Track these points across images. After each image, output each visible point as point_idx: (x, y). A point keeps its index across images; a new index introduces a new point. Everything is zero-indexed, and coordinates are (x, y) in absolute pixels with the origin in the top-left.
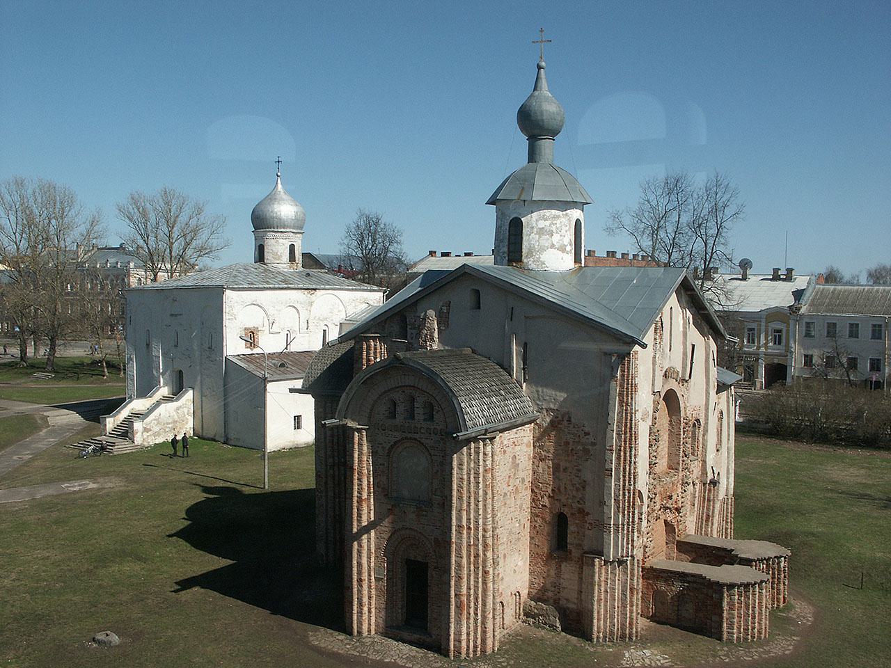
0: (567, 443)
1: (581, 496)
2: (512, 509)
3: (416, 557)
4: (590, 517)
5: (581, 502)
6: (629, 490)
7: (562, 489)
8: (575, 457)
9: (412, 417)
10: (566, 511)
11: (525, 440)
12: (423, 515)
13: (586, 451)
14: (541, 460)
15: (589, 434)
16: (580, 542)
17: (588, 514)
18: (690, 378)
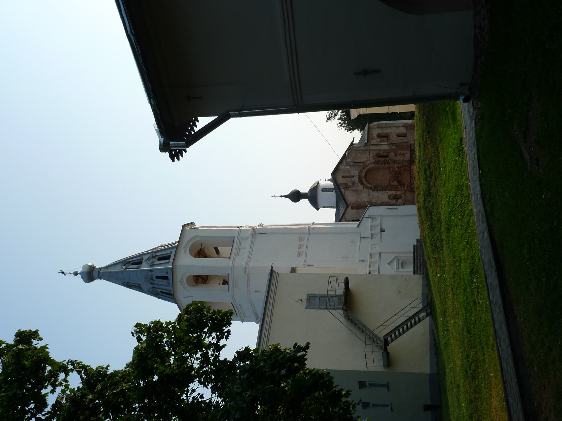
18: (363, 163)
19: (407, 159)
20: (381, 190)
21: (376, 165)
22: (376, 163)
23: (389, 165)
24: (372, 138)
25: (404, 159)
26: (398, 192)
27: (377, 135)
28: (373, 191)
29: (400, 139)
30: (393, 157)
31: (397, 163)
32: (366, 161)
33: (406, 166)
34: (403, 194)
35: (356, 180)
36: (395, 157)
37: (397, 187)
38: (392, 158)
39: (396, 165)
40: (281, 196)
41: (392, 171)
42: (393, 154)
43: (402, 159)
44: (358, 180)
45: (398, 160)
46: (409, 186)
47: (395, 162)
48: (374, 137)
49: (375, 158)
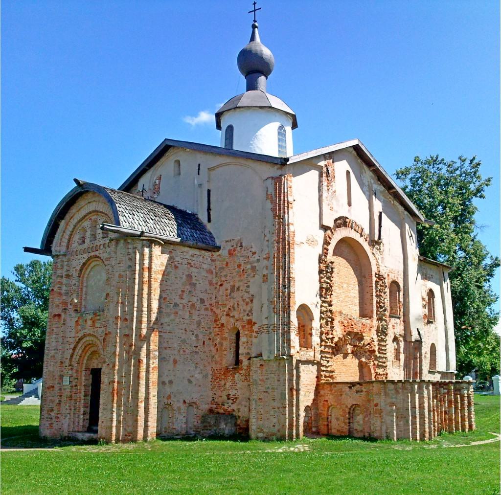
0: (239, 266)
1: (249, 309)
2: (186, 322)
3: (97, 365)
4: (257, 326)
5: (250, 314)
6: (284, 293)
7: (236, 306)
8: (246, 276)
9: (95, 239)
10: (239, 325)
11: (205, 266)
12: (97, 320)
13: (253, 268)
14: (221, 285)
15: (255, 253)
16: (249, 351)
17: (255, 323)
18: (379, 238)
19: (388, 371)
20: (320, 282)
21: (374, 279)
22: (380, 277)
23: (375, 317)
26: (319, 341)
28: (320, 261)
30: (392, 330)
31: (382, 340)
32: (382, 250)
33: (375, 370)
34: (312, 354)
35: (343, 211)
37: (330, 336)
38: (390, 326)
39: (375, 337)
44: (345, 215)
45: (387, 343)
46: (331, 377)
47: (382, 332)
49: (388, 275)
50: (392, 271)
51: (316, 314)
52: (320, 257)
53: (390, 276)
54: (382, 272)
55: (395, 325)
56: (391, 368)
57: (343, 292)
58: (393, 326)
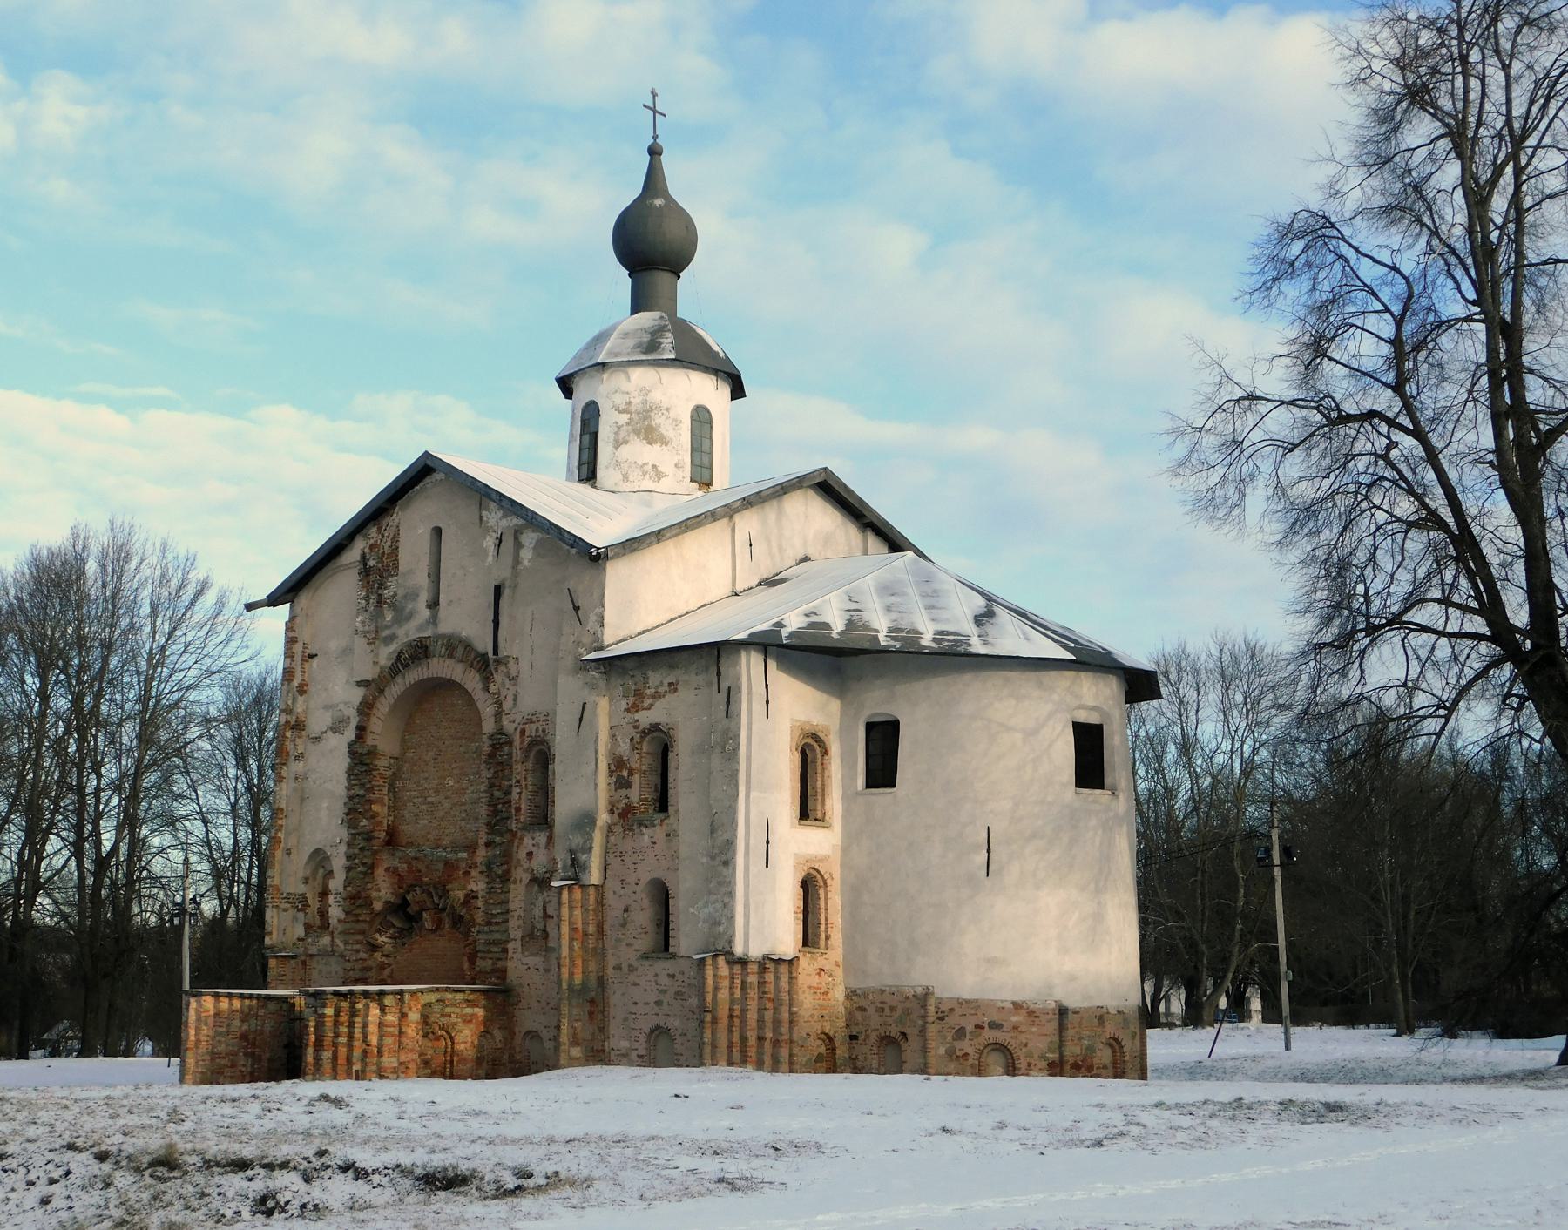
19: (510, 965)
24: (639, 695)
25: (510, 946)
27: (655, 727)
28: (352, 753)
29: (626, 910)
32: (513, 673)
36: (526, 877)
38: (522, 854)
39: (478, 885)
40: (654, 152)
41: (447, 863)
42: (540, 863)
43: (515, 928)
44: (414, 635)
48: (652, 705)
49: (523, 732)
50: (534, 719)
51: (338, 863)
52: (350, 745)
53: (527, 734)
54: (508, 726)
55: (534, 849)
56: (518, 955)
57: (446, 798)
58: (530, 854)
